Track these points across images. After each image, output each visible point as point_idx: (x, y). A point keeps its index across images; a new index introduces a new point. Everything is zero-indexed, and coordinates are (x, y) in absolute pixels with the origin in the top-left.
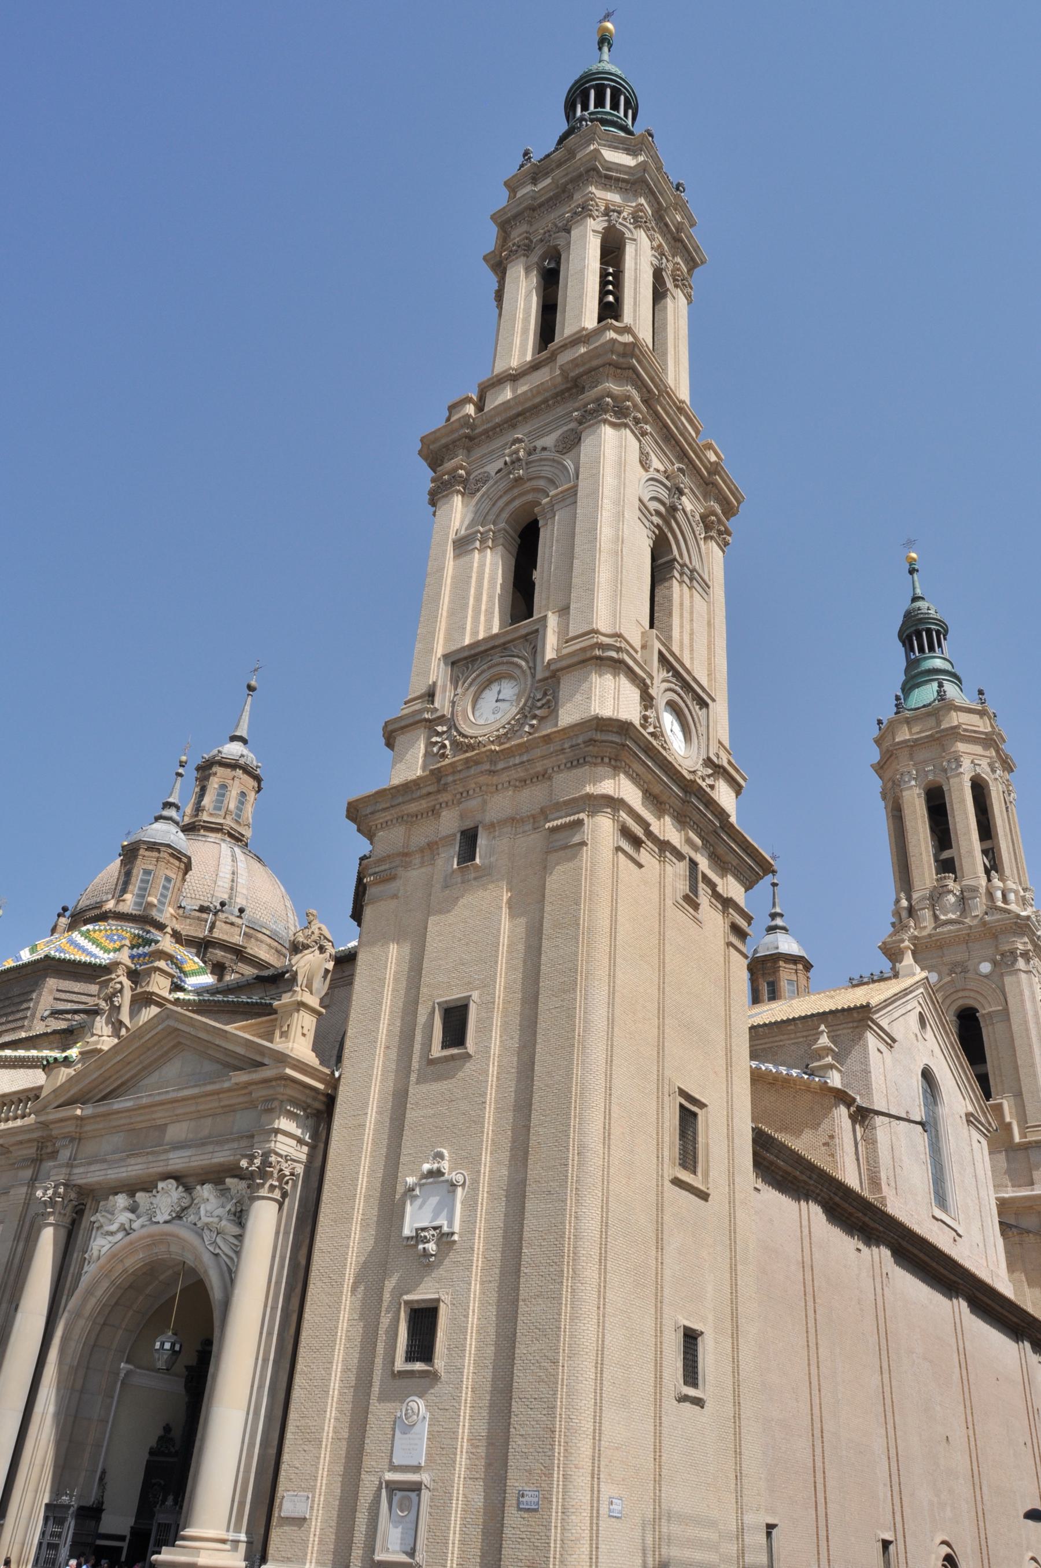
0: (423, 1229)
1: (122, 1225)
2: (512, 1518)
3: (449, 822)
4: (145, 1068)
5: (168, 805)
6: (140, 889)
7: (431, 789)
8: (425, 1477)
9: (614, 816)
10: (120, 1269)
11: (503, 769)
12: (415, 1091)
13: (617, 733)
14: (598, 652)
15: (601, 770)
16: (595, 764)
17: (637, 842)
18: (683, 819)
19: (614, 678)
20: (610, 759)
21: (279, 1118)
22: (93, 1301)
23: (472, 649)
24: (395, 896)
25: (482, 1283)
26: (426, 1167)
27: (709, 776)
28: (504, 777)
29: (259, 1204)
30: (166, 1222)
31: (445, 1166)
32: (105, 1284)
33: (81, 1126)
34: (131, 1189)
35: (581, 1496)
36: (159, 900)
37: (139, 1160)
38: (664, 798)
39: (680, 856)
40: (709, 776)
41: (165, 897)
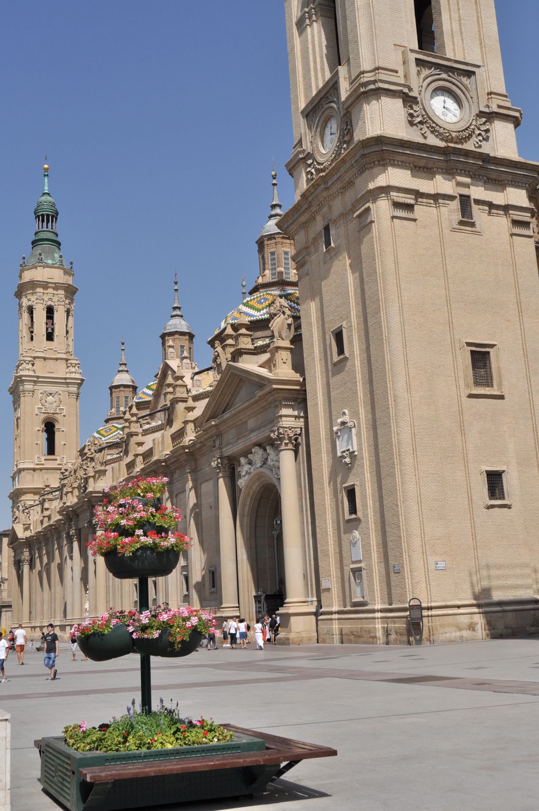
0: (344, 452)
1: (247, 471)
2: (393, 577)
3: (319, 225)
4: (233, 395)
5: (274, 207)
6: (272, 265)
7: (306, 206)
8: (362, 565)
9: (387, 197)
10: (252, 492)
11: (332, 184)
12: (332, 381)
13: (376, 144)
14: (362, 90)
15: (375, 170)
16: (372, 168)
17: (409, 207)
18: (451, 172)
19: (378, 101)
20: (379, 161)
21: (281, 410)
22: (247, 508)
23: (312, 103)
24: (308, 274)
25: (370, 473)
26: (339, 420)
27: (484, 123)
28: (334, 189)
29: (283, 453)
30: (261, 467)
31: (346, 418)
32: (249, 500)
33: (219, 429)
34: (246, 453)
35: (418, 563)
36: (285, 268)
37: (242, 440)
38: (430, 166)
39: (451, 198)
40: (484, 123)
41: (288, 264)
